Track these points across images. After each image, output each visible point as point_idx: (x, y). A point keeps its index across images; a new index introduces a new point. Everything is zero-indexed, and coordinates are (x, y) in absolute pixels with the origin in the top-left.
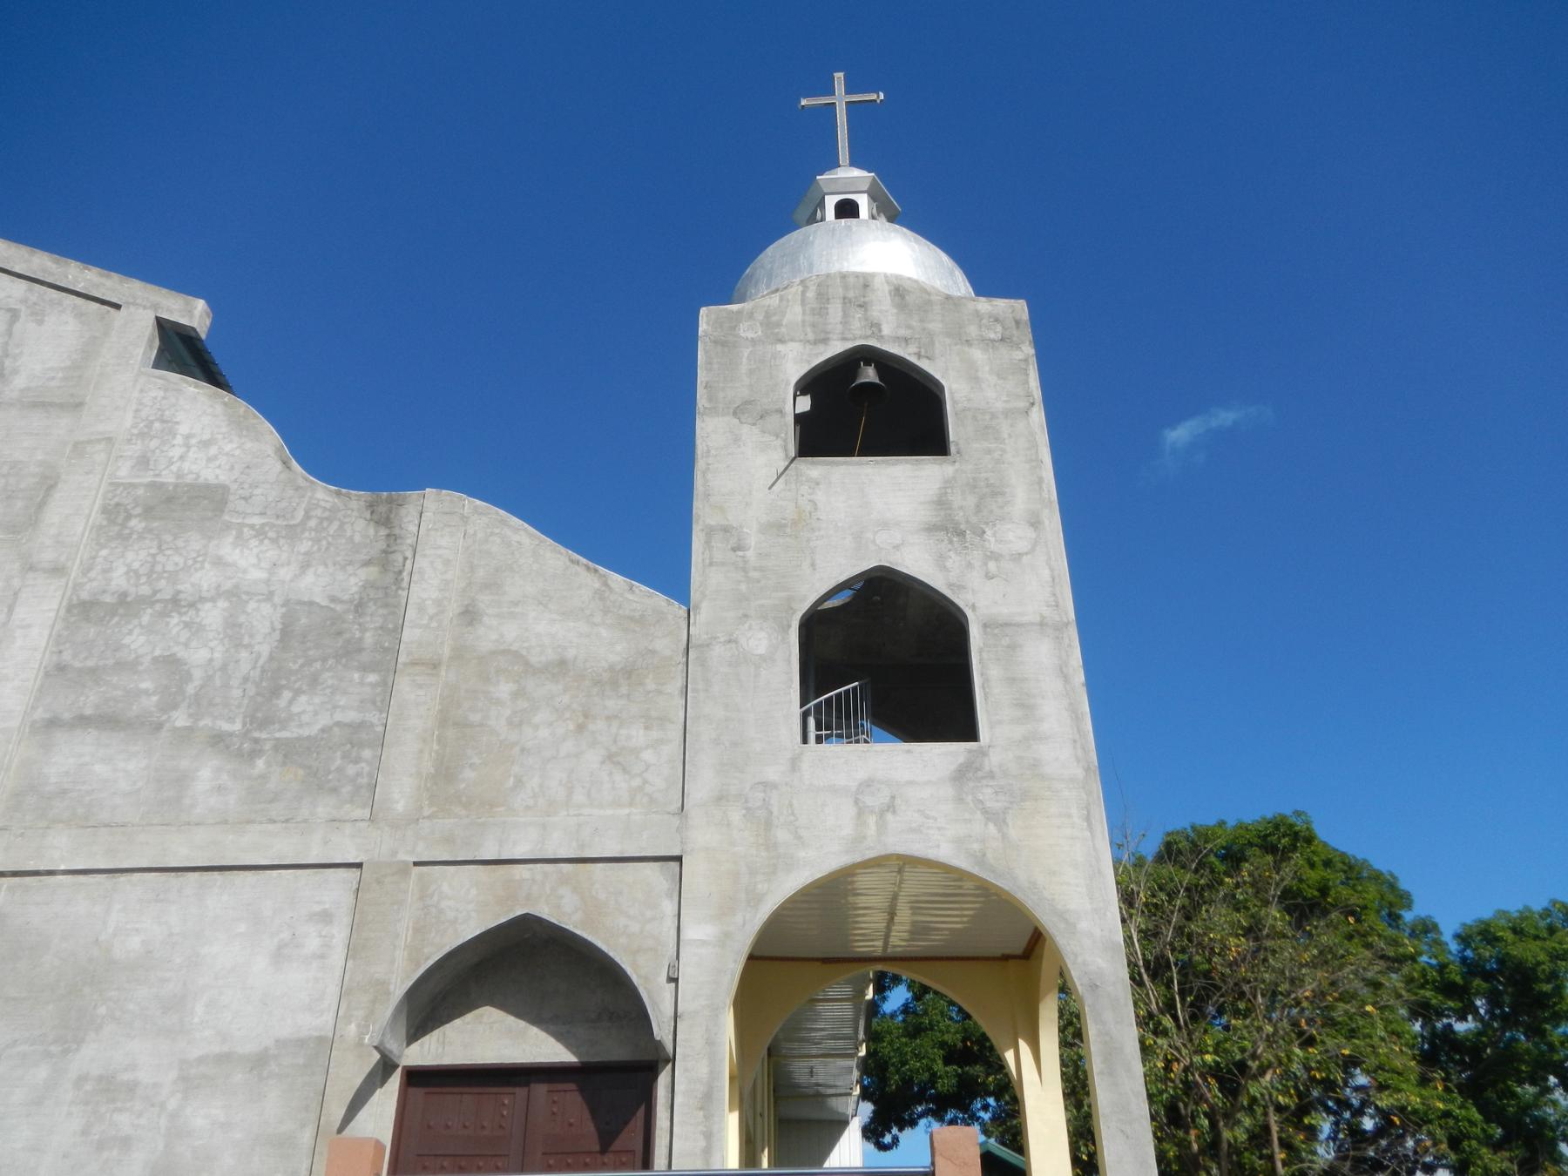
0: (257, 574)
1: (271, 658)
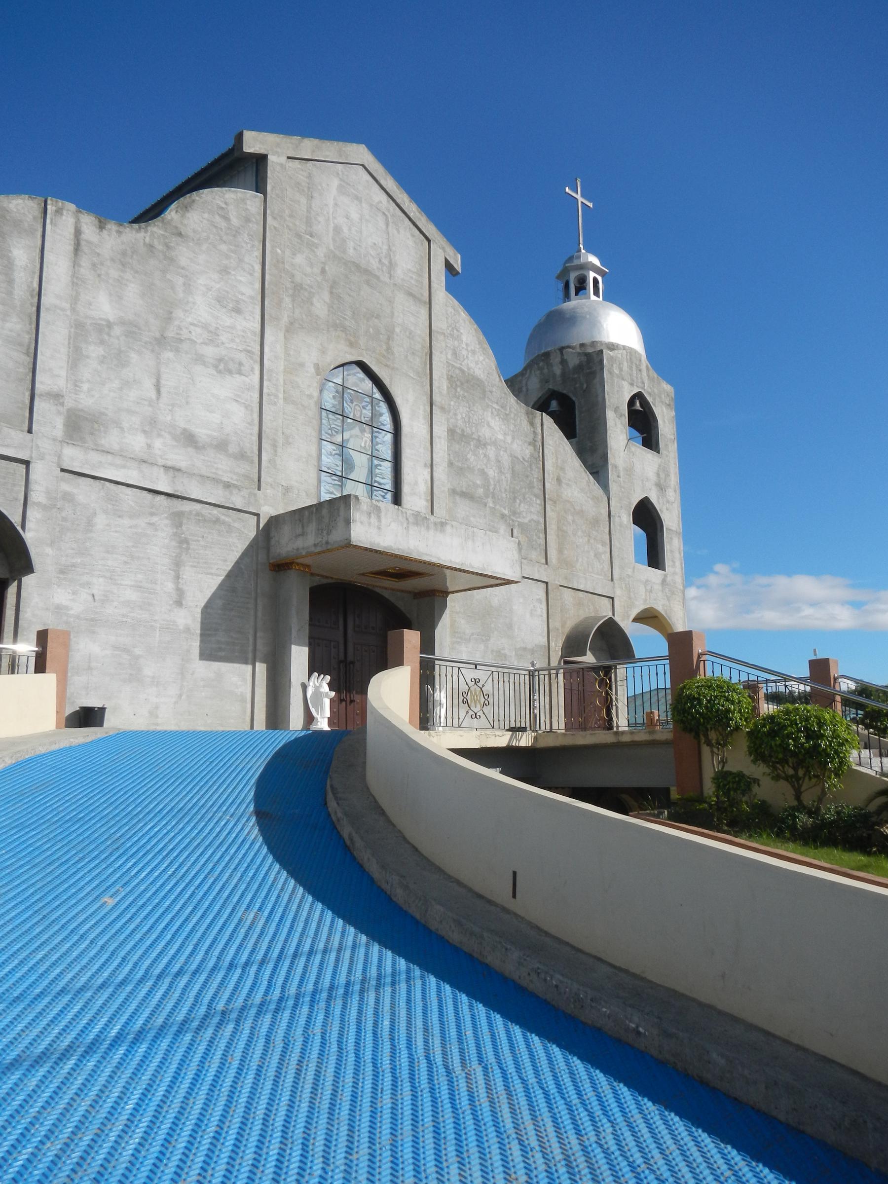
0: (500, 437)
1: (511, 483)
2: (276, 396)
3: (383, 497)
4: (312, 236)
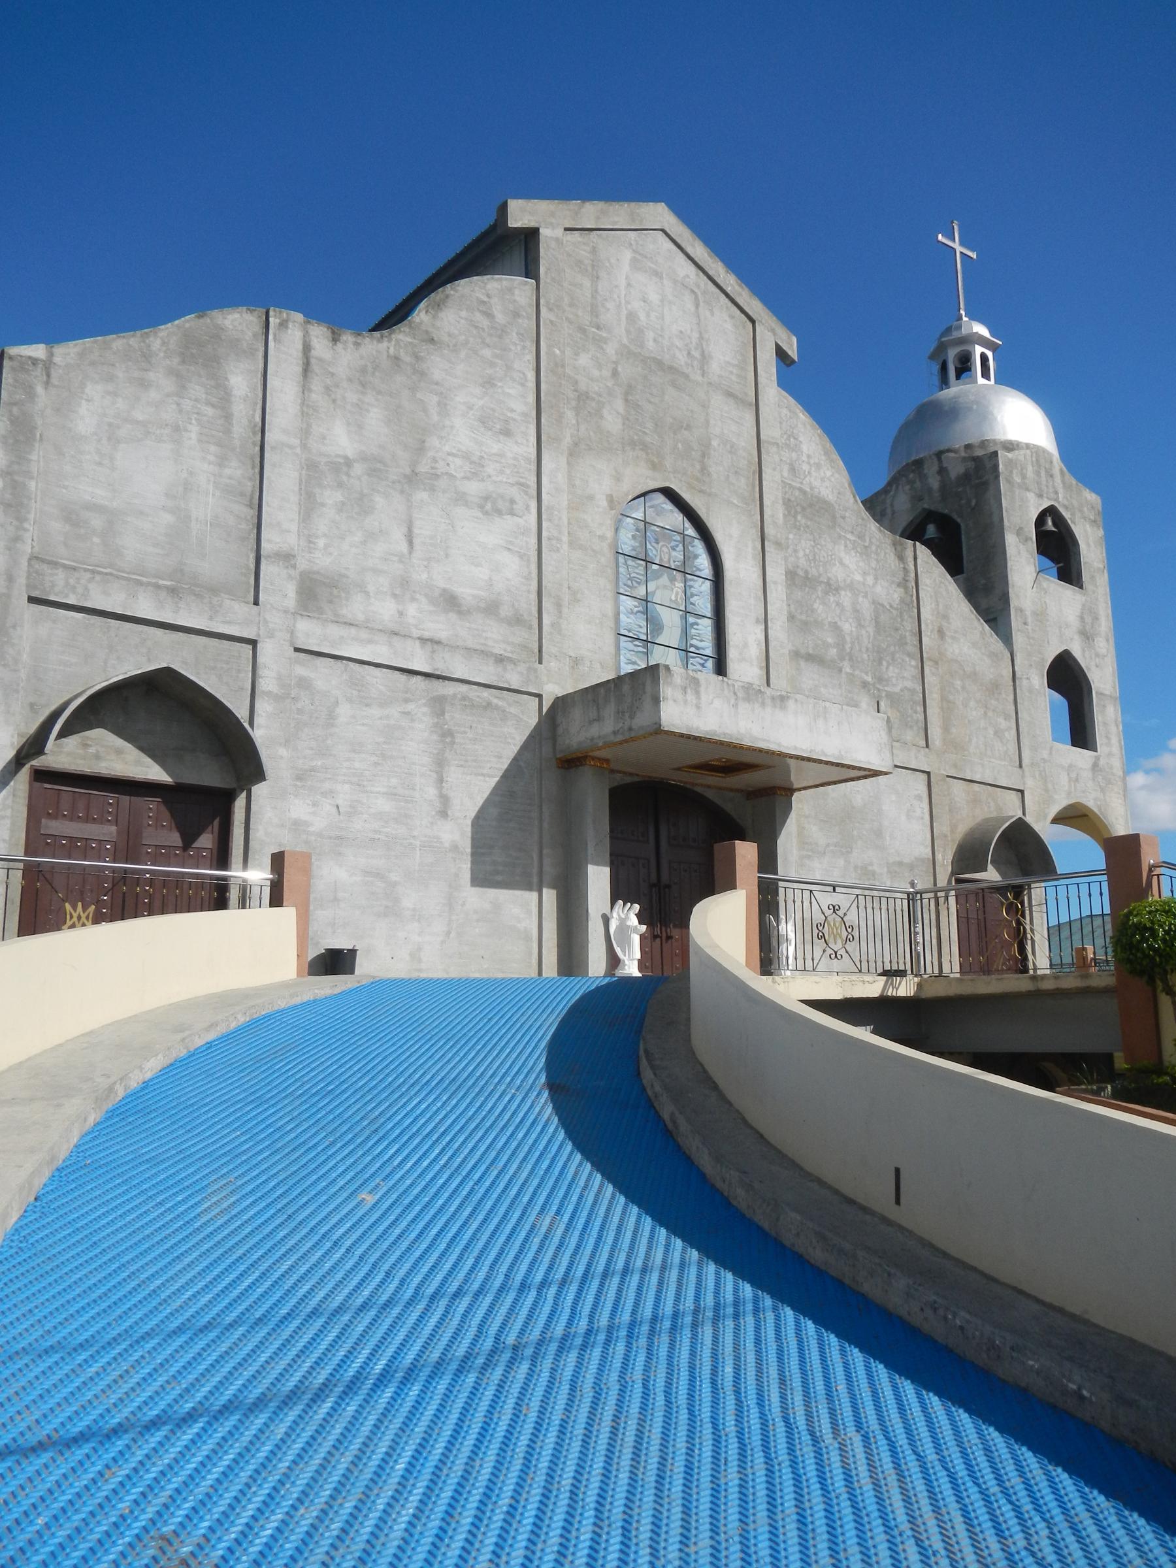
2: (559, 540)
3: (703, 665)
4: (598, 328)
